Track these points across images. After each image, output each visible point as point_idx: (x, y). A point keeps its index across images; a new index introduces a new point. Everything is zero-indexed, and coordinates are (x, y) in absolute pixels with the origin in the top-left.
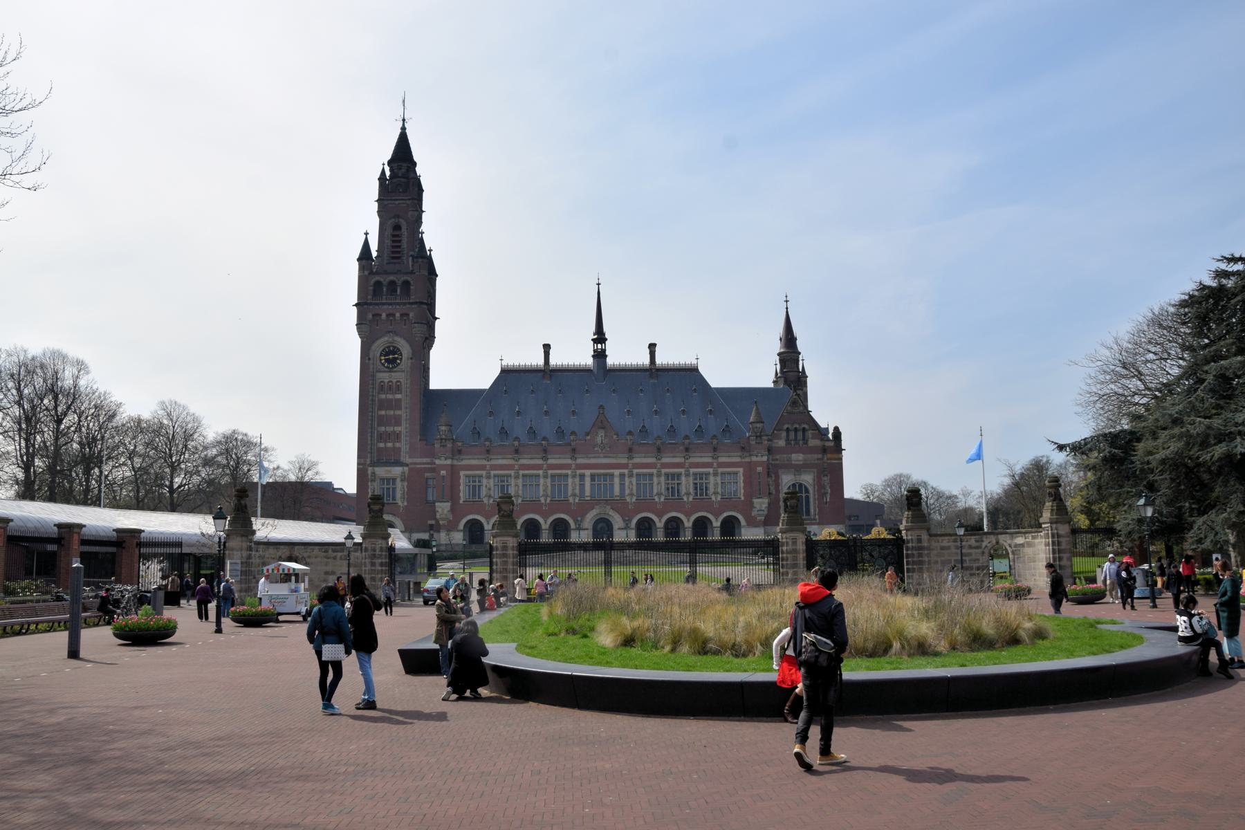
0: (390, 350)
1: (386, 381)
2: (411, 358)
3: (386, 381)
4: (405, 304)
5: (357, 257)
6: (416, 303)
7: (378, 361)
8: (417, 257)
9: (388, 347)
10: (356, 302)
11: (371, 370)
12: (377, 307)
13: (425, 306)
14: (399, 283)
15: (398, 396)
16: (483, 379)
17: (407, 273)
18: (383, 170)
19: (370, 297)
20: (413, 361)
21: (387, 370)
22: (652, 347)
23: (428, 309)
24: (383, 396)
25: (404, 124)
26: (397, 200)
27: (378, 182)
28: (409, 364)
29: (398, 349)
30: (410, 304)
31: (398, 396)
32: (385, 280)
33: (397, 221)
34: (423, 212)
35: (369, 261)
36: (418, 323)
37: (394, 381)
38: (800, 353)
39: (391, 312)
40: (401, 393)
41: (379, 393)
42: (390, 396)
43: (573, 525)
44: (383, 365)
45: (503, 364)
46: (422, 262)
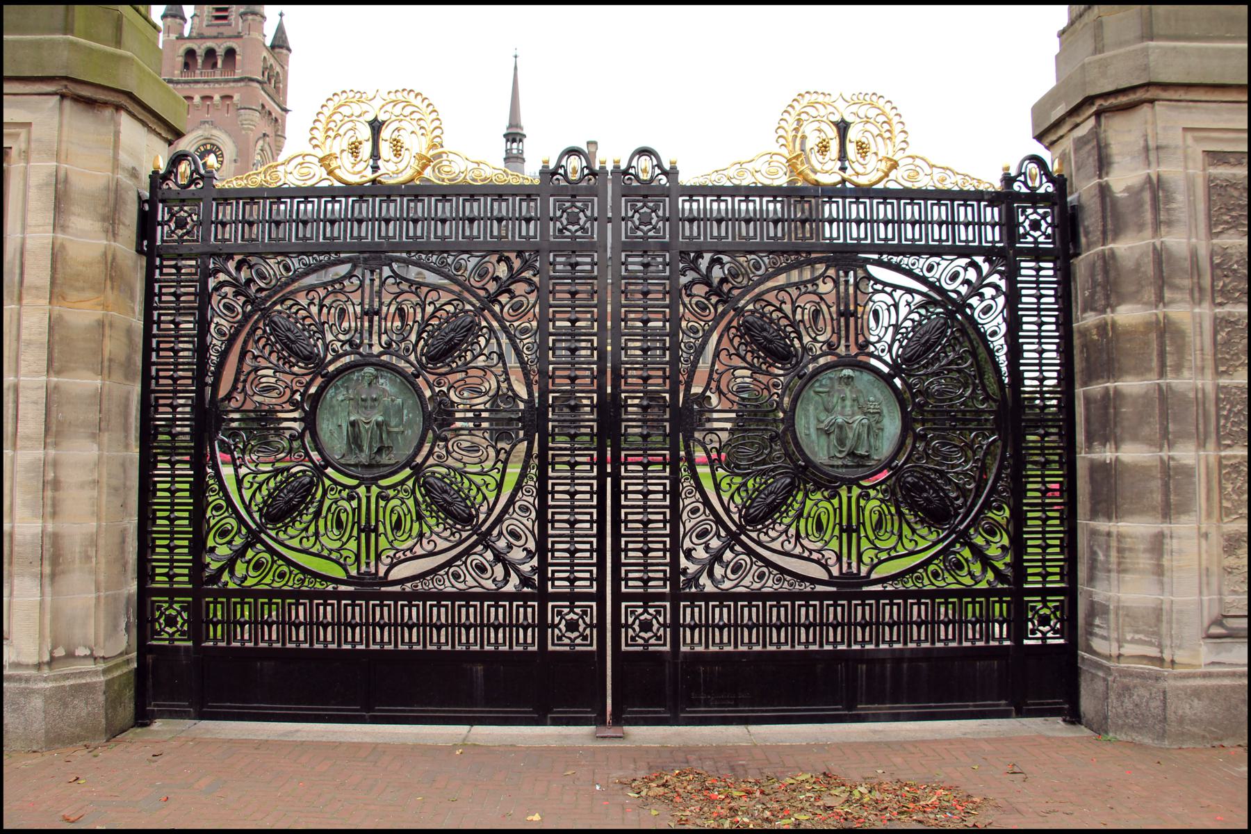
0: (206, 150)
2: (235, 161)
4: (227, 81)
6: (241, 80)
9: (203, 145)
12: (187, 86)
14: (220, 51)
17: (230, 37)
19: (177, 72)
20: (238, 164)
23: (263, 89)
29: (218, 147)
30: (235, 81)
32: (199, 48)
36: (245, 108)
39: (207, 93)
46: (253, 20)
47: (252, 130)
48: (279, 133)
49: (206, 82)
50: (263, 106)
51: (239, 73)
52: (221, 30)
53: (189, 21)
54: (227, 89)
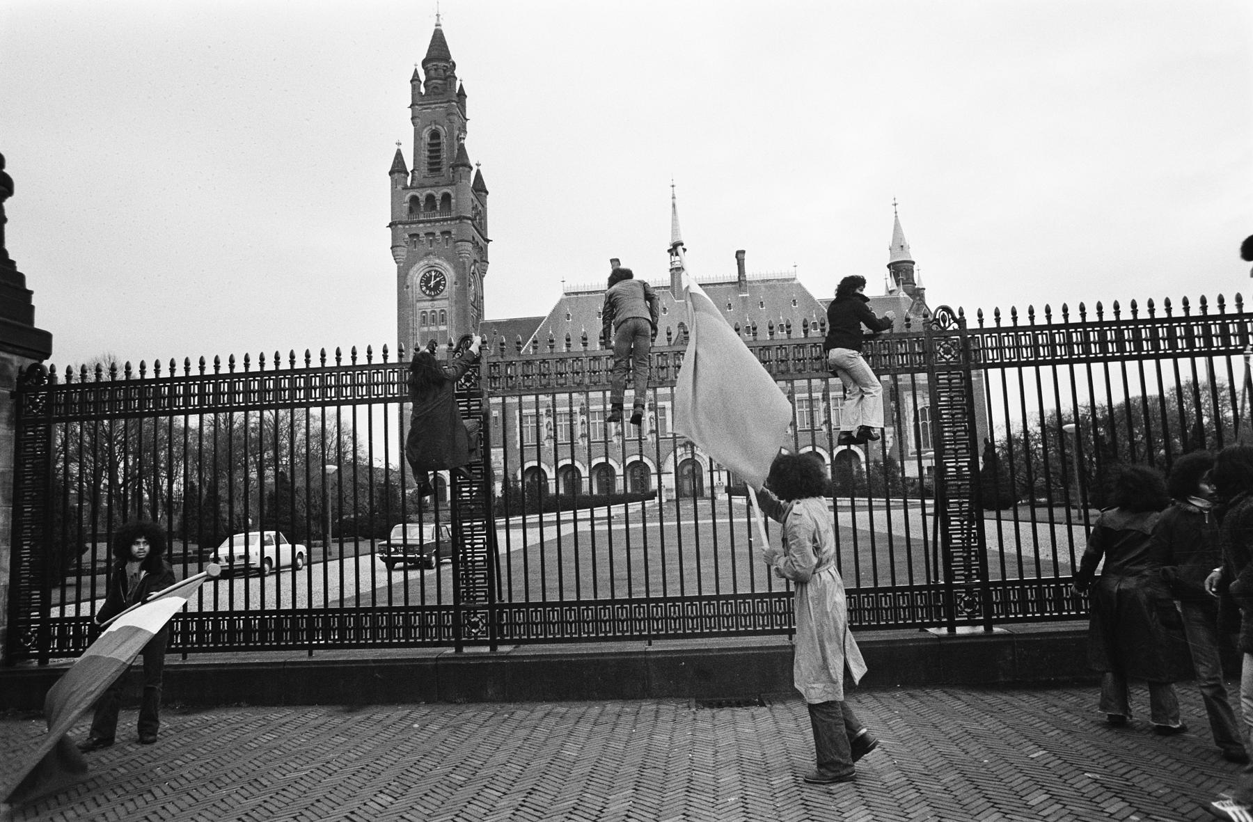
1: (428, 311)
2: (456, 283)
3: (428, 311)
5: (389, 170)
7: (419, 288)
8: (458, 166)
9: (428, 272)
10: (390, 221)
11: (410, 299)
13: (470, 222)
14: (438, 196)
15: (443, 328)
16: (540, 306)
18: (416, 70)
21: (428, 298)
22: (740, 255)
23: (474, 225)
24: (426, 329)
25: (438, 20)
26: (435, 103)
27: (410, 85)
28: (454, 289)
31: (443, 328)
32: (421, 195)
33: (434, 128)
34: (467, 120)
35: (403, 175)
37: (438, 310)
38: (913, 263)
39: (430, 230)
40: (446, 324)
41: (421, 326)
42: (433, 329)
43: (653, 469)
44: (424, 292)
45: (566, 286)
47: (468, 258)
48: (484, 259)
49: (430, 221)
50: (473, 238)
51: (454, 214)
52: (437, 179)
53: (410, 174)
54: (446, 226)
